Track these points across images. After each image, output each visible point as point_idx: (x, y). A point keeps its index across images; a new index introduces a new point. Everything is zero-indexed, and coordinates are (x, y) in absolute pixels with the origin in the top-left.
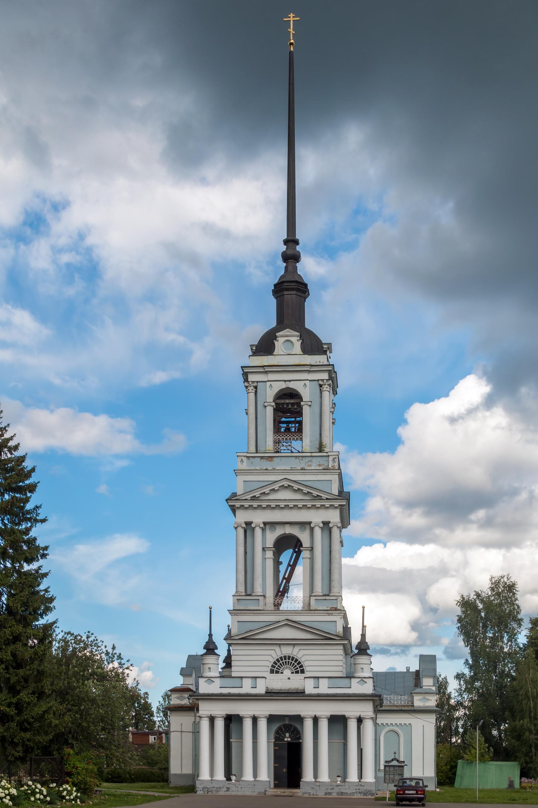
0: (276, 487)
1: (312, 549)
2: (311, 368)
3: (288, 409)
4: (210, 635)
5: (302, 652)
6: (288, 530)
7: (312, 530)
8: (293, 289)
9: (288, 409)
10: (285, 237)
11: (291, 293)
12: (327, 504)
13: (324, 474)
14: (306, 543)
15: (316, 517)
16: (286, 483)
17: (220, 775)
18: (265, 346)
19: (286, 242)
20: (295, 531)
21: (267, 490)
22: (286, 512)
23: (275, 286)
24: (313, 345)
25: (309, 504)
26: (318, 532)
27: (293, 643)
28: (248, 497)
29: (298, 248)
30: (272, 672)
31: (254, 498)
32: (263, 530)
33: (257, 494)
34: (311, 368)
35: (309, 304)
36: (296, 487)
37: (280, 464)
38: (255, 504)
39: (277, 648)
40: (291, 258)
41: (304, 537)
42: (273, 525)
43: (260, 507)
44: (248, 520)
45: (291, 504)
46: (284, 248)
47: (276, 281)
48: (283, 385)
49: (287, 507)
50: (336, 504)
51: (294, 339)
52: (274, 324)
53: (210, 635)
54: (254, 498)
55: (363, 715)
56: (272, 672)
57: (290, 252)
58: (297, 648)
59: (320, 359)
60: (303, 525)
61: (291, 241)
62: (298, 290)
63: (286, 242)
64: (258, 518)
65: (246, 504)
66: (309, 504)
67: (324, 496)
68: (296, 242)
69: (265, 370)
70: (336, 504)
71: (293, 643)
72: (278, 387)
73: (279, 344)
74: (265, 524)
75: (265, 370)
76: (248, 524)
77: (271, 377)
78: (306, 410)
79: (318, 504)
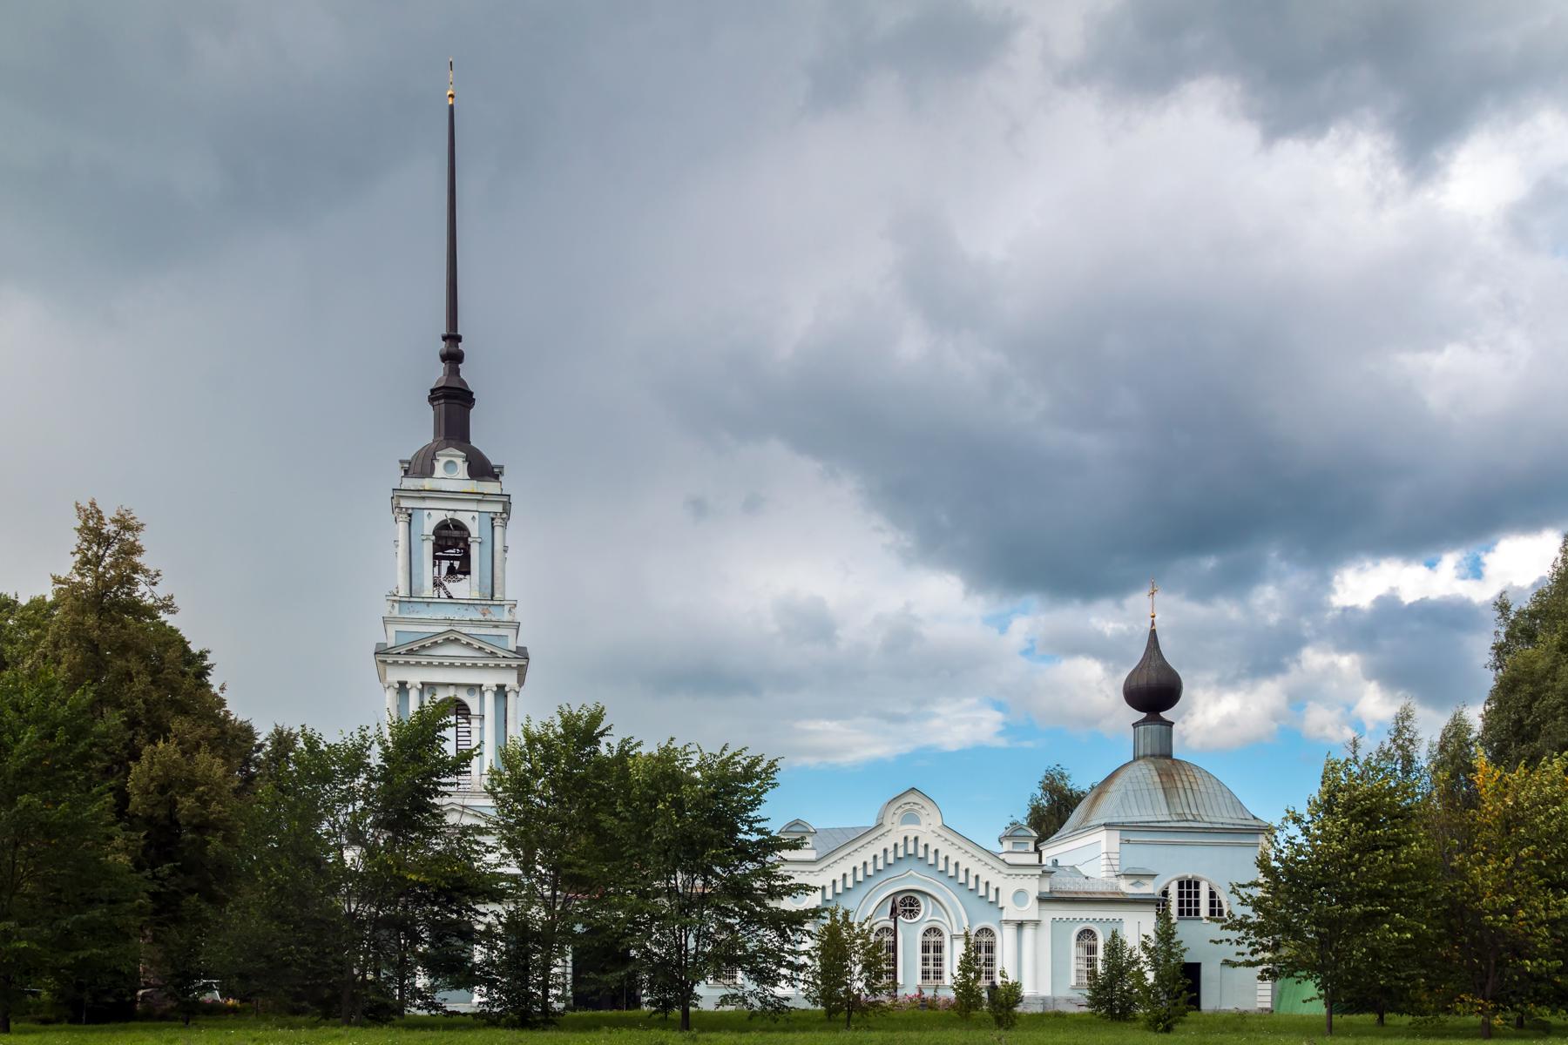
0: (440, 640)
1: (482, 717)
2: (482, 498)
3: (452, 544)
6: (451, 693)
7: (482, 694)
9: (452, 544)
12: (503, 663)
14: (475, 710)
15: (490, 680)
18: (421, 466)
19: (445, 338)
20: (463, 695)
21: (428, 643)
23: (433, 391)
24: (481, 469)
25: (480, 663)
26: (489, 698)
28: (403, 651)
31: (411, 652)
32: (421, 692)
33: (415, 647)
34: (482, 498)
38: (413, 660)
40: (453, 358)
41: (472, 702)
43: (418, 664)
44: (402, 679)
45: (457, 662)
47: (433, 386)
48: (450, 515)
50: (514, 663)
52: (429, 438)
57: (453, 349)
59: (489, 487)
61: (453, 338)
64: (415, 677)
65: (401, 660)
66: (480, 663)
67: (501, 654)
68: (459, 339)
73: (439, 467)
76: (403, 684)
77: (428, 504)
79: (492, 663)
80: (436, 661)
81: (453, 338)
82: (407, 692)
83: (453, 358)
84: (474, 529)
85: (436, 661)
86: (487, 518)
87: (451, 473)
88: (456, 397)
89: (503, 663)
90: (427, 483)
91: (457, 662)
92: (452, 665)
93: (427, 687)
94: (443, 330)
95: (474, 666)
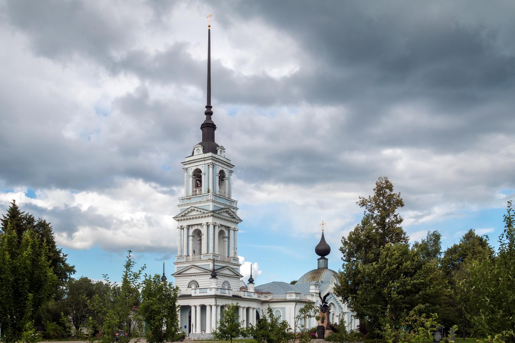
2: (204, 159)
5: (198, 278)
11: (209, 128)
12: (206, 215)
13: (207, 202)
15: (204, 221)
16: (193, 208)
17: (199, 331)
19: (206, 107)
20: (199, 228)
21: (186, 212)
22: (194, 220)
26: (205, 227)
27: (195, 275)
28: (180, 216)
29: (212, 110)
30: (188, 287)
31: (182, 216)
32: (188, 229)
34: (204, 159)
35: (216, 132)
36: (196, 209)
37: (193, 201)
38: (183, 218)
40: (209, 113)
42: (192, 225)
43: (184, 219)
45: (197, 216)
46: (206, 109)
48: (195, 168)
49: (196, 218)
50: (210, 214)
51: (200, 148)
54: (182, 216)
55: (211, 304)
56: (188, 287)
57: (209, 111)
58: (196, 277)
60: (201, 224)
61: (209, 107)
62: (207, 127)
63: (206, 107)
68: (211, 107)
69: (190, 162)
70: (210, 214)
71: (195, 275)
74: (189, 226)
75: (190, 162)
78: (203, 176)
80: (191, 217)
81: (209, 107)
82: (183, 229)
83: (209, 113)
84: (203, 172)
85: (191, 217)
86: (207, 165)
87: (199, 154)
88: (211, 127)
89: (206, 215)
92: (196, 218)
94: (206, 104)
95: (199, 217)
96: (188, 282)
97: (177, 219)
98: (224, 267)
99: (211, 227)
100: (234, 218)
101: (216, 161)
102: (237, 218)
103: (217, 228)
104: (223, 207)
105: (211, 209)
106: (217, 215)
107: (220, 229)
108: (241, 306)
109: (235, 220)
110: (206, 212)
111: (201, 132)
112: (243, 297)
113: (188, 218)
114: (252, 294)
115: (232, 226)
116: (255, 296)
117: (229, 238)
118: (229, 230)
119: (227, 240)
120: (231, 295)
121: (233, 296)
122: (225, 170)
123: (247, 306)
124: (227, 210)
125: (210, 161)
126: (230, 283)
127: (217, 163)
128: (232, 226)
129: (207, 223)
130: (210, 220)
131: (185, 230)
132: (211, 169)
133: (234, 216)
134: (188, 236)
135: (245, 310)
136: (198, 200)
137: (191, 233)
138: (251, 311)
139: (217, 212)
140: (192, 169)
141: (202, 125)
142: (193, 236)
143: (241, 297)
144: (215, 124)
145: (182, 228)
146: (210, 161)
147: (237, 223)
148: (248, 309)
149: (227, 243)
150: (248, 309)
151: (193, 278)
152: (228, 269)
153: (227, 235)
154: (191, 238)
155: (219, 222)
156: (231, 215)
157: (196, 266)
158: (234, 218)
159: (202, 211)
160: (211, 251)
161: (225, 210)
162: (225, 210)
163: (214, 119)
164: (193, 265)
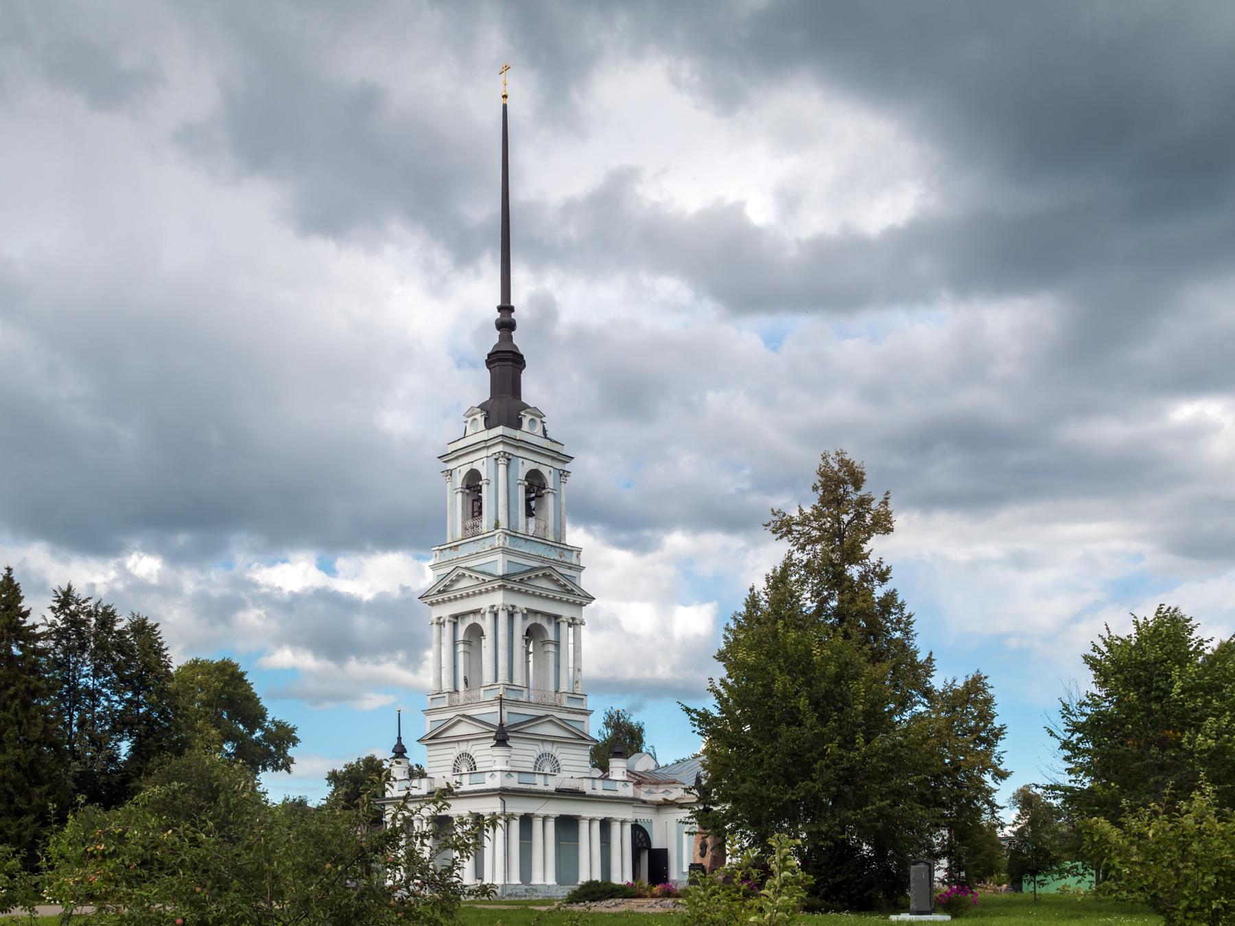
2: (486, 444)
4: (399, 739)
8: (507, 360)
10: (499, 304)
11: (506, 363)
15: (484, 603)
16: (460, 571)
19: (500, 309)
21: (447, 582)
26: (489, 618)
31: (439, 592)
32: (455, 624)
36: (467, 573)
38: (440, 598)
39: (456, 745)
45: (470, 591)
46: (498, 315)
50: (496, 585)
51: (478, 417)
53: (399, 739)
54: (439, 592)
57: (506, 319)
58: (471, 743)
61: (506, 308)
62: (500, 360)
63: (500, 309)
68: (511, 309)
72: (530, 466)
74: (456, 617)
78: (484, 488)
82: (443, 623)
86: (492, 460)
90: (518, 434)
91: (470, 591)
93: (456, 618)
95: (474, 594)
96: (453, 758)
97: (428, 601)
98: (540, 717)
99: (503, 617)
100: (571, 592)
101: (518, 447)
102: (577, 592)
103: (518, 619)
104: (535, 564)
105: (500, 573)
106: (516, 587)
107: (531, 621)
108: (584, 815)
109: (572, 599)
110: (487, 578)
111: (486, 374)
112: (589, 791)
113: (452, 596)
114: (619, 786)
115: (566, 612)
116: (629, 791)
117: (557, 644)
118: (558, 624)
119: (551, 648)
120: (552, 788)
121: (557, 790)
122: (545, 471)
123: (602, 816)
124: (548, 572)
125: (500, 448)
126: (559, 758)
127: (520, 453)
128: (566, 612)
129: (493, 607)
130: (498, 599)
131: (448, 628)
132: (502, 468)
133: (570, 587)
134: (455, 643)
135: (596, 827)
136: (473, 548)
137: (461, 635)
138: (616, 829)
139: (517, 579)
140: (461, 469)
141: (489, 355)
142: (464, 642)
143: (582, 794)
144: (522, 352)
145: (440, 623)
146: (500, 448)
147: (581, 605)
148: (605, 824)
149: (551, 657)
150: (605, 824)
151: (463, 747)
152: (550, 721)
153: (551, 635)
154: (461, 648)
155: (522, 603)
156: (561, 586)
157: (469, 717)
158: (571, 592)
159: (481, 577)
160: (503, 677)
161: (540, 573)
162: (540, 573)
163: (519, 339)
164: (464, 716)
